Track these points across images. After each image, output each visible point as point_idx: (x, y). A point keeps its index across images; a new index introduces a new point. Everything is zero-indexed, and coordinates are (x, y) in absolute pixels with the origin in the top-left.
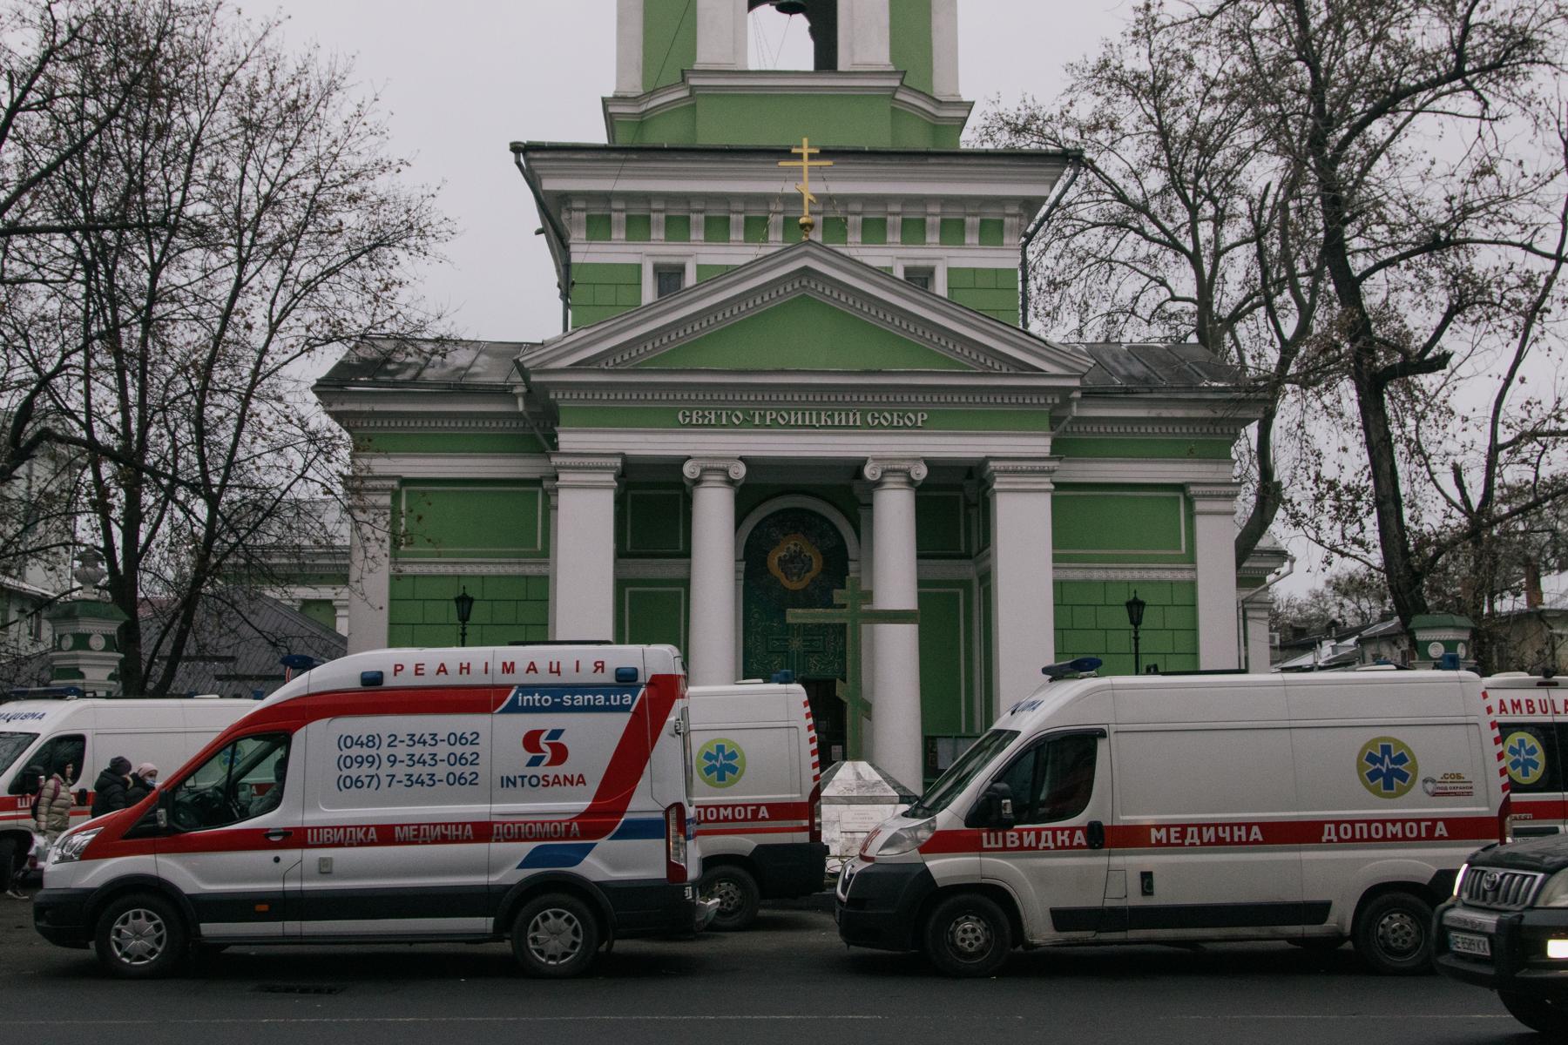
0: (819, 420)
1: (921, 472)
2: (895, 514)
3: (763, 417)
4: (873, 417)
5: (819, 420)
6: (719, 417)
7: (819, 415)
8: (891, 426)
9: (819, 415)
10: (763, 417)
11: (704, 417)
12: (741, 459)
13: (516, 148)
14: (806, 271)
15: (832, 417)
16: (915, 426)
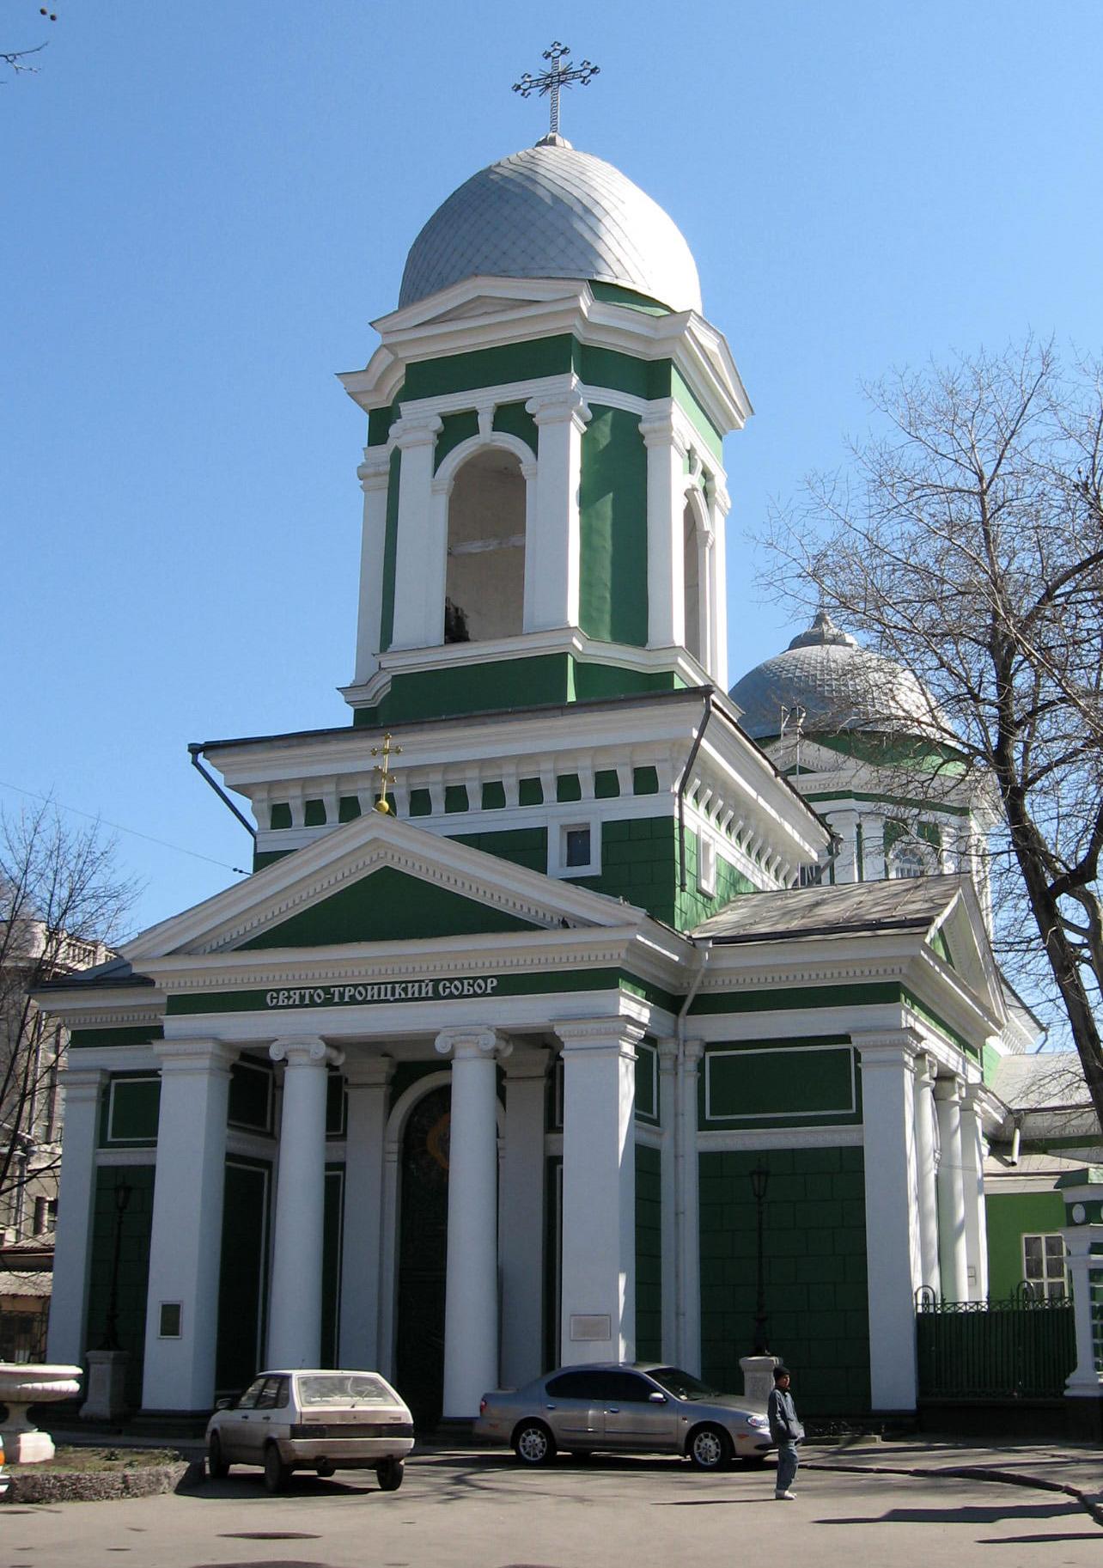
0: (393, 994)
1: (491, 1041)
2: (471, 1090)
3: (342, 995)
4: (445, 988)
5: (393, 994)
6: (302, 997)
7: (393, 989)
8: (461, 996)
9: (393, 989)
10: (342, 995)
11: (289, 998)
12: (323, 1038)
13: (195, 749)
14: (375, 840)
15: (405, 990)
16: (484, 995)
